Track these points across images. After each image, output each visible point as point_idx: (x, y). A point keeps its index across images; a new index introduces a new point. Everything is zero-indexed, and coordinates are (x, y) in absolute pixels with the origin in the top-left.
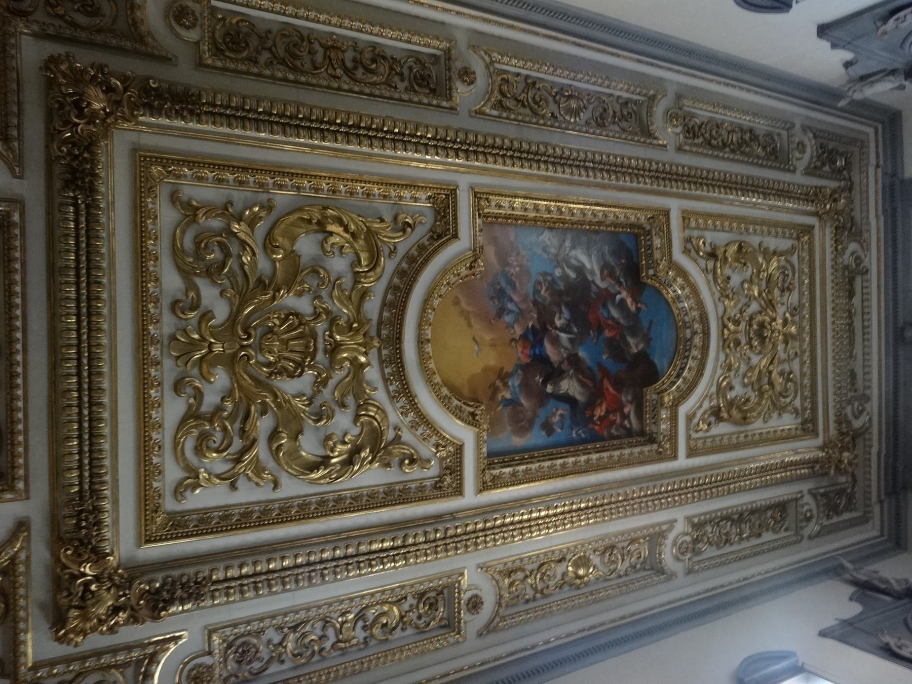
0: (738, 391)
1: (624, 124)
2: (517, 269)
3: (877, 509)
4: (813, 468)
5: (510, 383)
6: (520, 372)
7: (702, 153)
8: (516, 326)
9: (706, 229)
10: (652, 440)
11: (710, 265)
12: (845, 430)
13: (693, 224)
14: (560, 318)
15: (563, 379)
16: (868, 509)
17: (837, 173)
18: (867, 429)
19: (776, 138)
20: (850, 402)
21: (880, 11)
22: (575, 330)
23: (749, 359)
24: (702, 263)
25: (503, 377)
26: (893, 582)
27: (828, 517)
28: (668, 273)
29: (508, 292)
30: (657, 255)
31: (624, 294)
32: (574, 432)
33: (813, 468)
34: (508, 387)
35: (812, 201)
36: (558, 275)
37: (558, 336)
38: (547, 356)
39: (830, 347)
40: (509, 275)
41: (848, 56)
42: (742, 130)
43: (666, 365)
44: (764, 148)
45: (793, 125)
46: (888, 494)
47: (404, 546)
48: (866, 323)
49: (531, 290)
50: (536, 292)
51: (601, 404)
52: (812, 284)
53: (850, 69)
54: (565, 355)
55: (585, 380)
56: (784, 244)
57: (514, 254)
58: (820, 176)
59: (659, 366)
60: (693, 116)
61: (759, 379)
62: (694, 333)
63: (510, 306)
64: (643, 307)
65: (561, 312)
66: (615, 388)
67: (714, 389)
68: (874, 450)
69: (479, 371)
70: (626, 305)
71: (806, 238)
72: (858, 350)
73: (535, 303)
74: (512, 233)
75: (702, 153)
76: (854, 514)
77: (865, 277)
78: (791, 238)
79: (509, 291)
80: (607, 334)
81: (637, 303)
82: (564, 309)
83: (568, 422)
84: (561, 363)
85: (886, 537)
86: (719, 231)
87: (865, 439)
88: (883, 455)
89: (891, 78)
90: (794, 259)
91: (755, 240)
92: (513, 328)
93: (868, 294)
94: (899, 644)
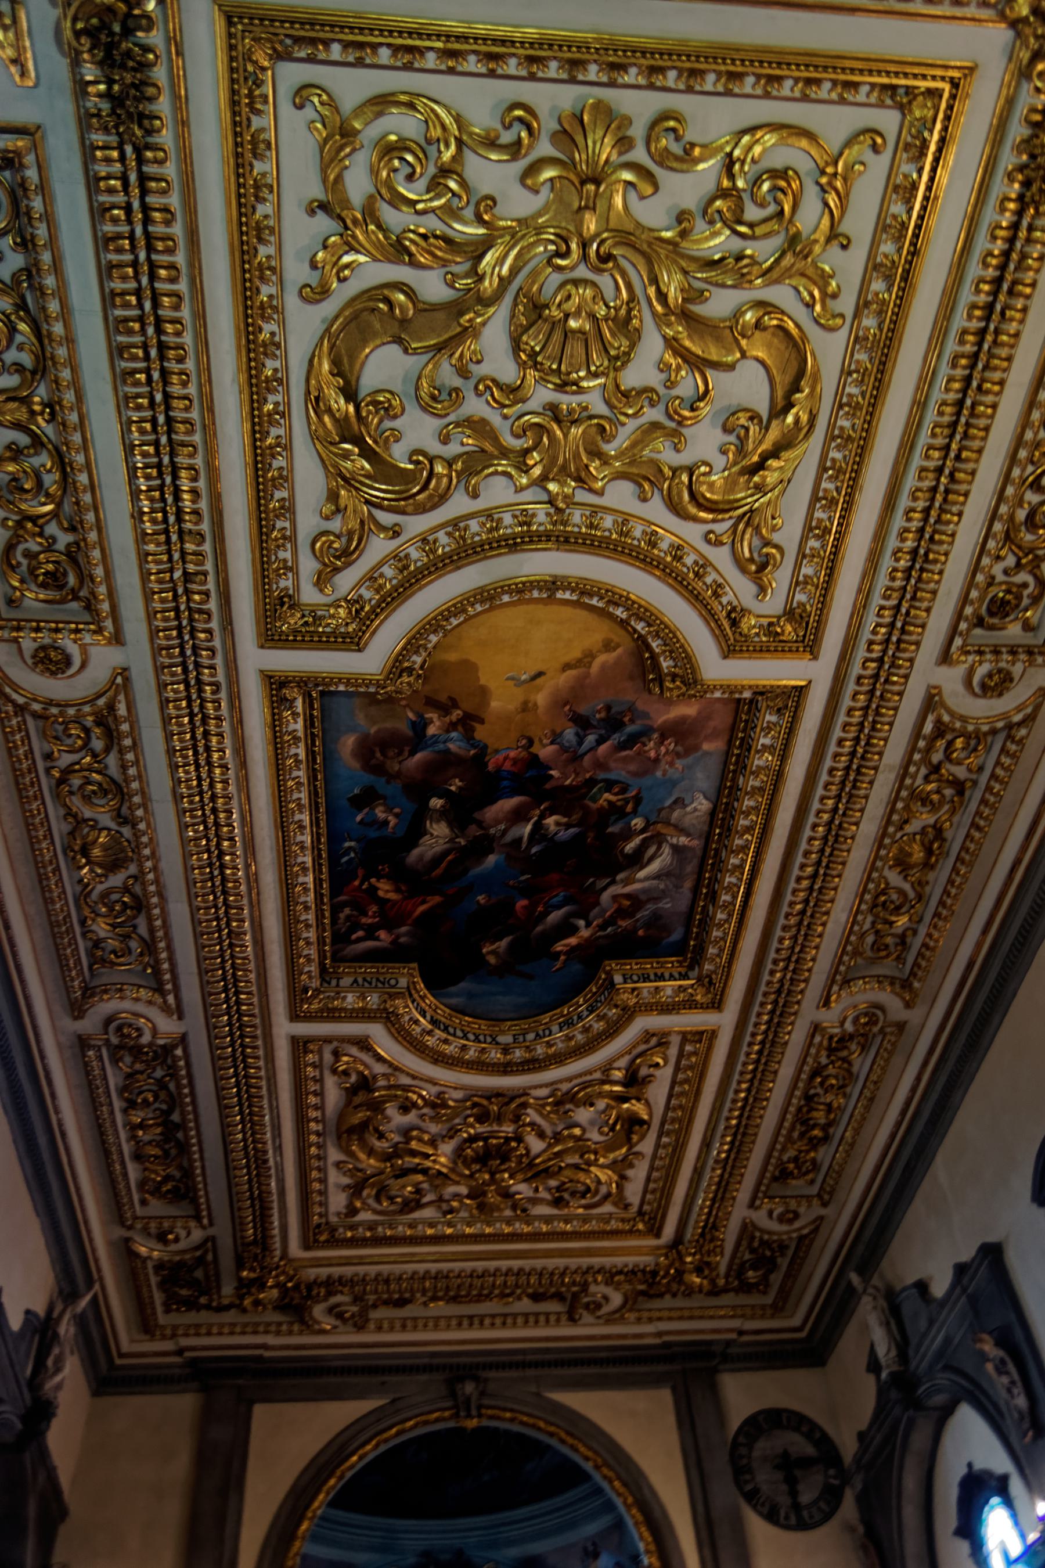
0: (396, 1118)
1: (870, 939)
2: (652, 754)
3: (168, 1346)
4: (255, 1242)
5: (454, 734)
6: (472, 752)
7: (804, 1062)
9: (677, 1069)
11: (618, 1075)
12: (315, 1292)
13: (688, 1048)
14: (558, 824)
15: (450, 825)
16: (168, 1332)
17: (737, 1270)
19: (810, 1176)
20: (357, 1299)
21: (1019, 1335)
22: (534, 850)
23: (451, 1138)
25: (468, 722)
26: (58, 1379)
28: (616, 1006)
29: (616, 736)
31: (585, 933)
32: (353, 844)
34: (448, 731)
35: (702, 1235)
37: (529, 821)
39: (457, 1266)
40: (644, 739)
41: (939, 1289)
42: (830, 1124)
43: (453, 1001)
44: (795, 1160)
45: (825, 1205)
47: (181, 533)
48: (487, 1321)
49: (612, 776)
50: (609, 785)
51: (397, 890)
52: (564, 1236)
53: (914, 1291)
55: (443, 865)
56: (633, 1192)
57: (679, 749)
59: (453, 989)
60: (864, 1048)
61: (414, 1153)
62: (506, 1050)
63: (591, 738)
64: (558, 965)
65: (568, 826)
66: (423, 913)
67: (405, 1080)
68: (271, 1340)
69: (482, 682)
71: (641, 1226)
72: (438, 1308)
73: (592, 782)
75: (804, 1062)
76: (159, 1309)
77: (564, 1318)
78: (642, 1202)
79: (616, 738)
81: (566, 953)
82: (573, 831)
83: (373, 834)
84: (480, 824)
86: (672, 1088)
87: (291, 1323)
89: (893, 1353)
91: (646, 1146)
92: (552, 743)
93: (537, 1322)
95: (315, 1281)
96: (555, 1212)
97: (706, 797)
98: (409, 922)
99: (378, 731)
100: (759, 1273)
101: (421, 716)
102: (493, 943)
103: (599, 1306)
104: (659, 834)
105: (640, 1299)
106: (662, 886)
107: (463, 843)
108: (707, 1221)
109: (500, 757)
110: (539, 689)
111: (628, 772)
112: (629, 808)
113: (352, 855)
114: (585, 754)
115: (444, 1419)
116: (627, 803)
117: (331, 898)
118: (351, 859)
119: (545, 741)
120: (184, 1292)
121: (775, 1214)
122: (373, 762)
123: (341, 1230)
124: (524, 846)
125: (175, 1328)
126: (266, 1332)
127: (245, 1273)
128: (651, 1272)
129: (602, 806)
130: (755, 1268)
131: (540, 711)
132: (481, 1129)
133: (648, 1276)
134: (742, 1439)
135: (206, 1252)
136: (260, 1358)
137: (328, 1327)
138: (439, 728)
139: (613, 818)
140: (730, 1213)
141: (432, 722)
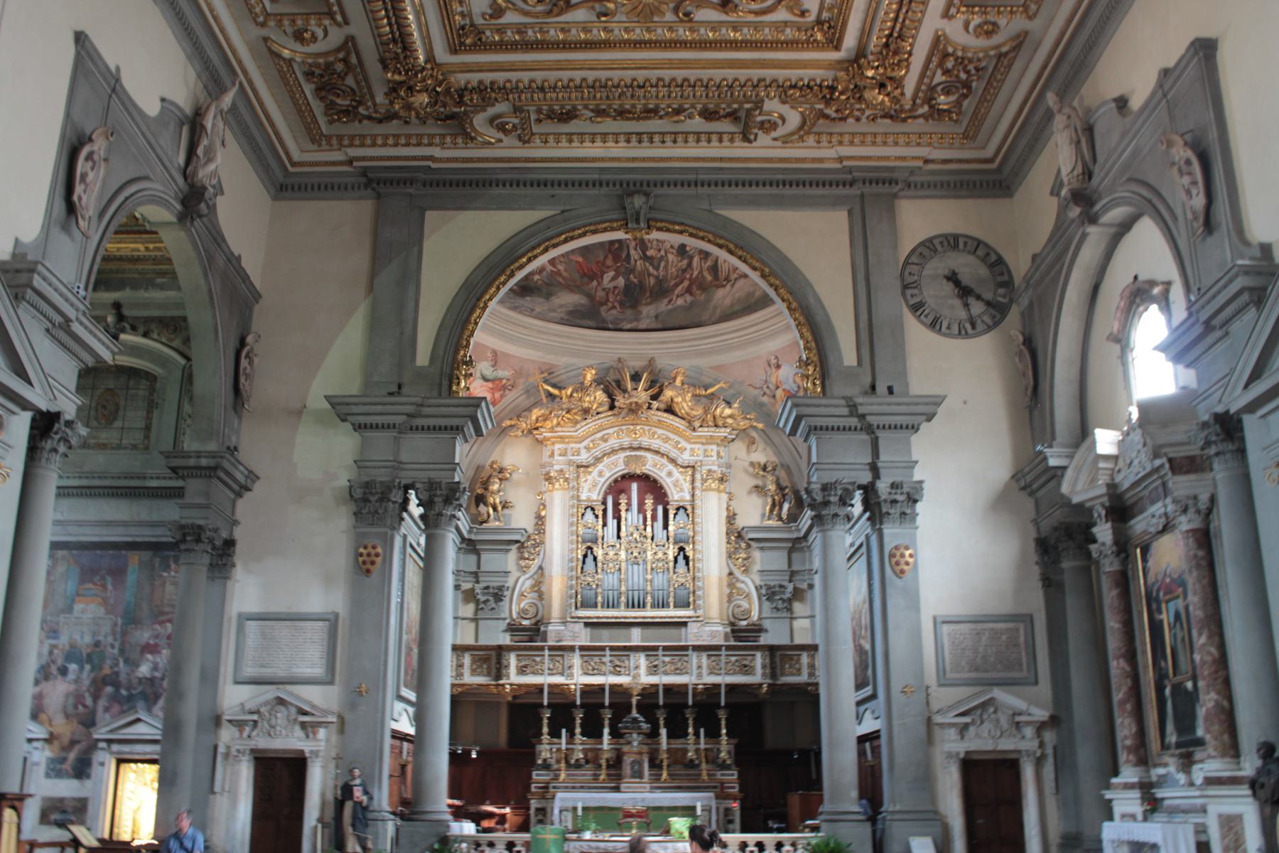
3: (337, 156)
4: (394, 41)
16: (334, 141)
18: (472, 139)
20: (517, 110)
21: (1213, 134)
26: (212, 167)
27: (309, 75)
33: (394, 41)
35: (887, 45)
46: (364, 172)
48: (656, 138)
53: (1113, 105)
58: (928, 61)
68: (437, 152)
71: (819, 36)
72: (609, 125)
76: (322, 120)
77: (738, 138)
85: (290, 169)
87: (455, 136)
88: (429, 163)
89: (1079, 170)
90: (781, 15)
94: (96, 157)
95: (466, 89)
96: (723, 17)
100: (952, 98)
103: (774, 126)
105: (821, 121)
108: (893, 28)
115: (613, 229)
120: (339, 101)
121: (971, 28)
123: (488, 33)
125: (340, 138)
126: (430, 145)
127: (389, 75)
128: (828, 87)
130: (947, 92)
133: (826, 91)
134: (914, 259)
135: (348, 54)
136: (430, 167)
137: (493, 141)
140: (920, 21)
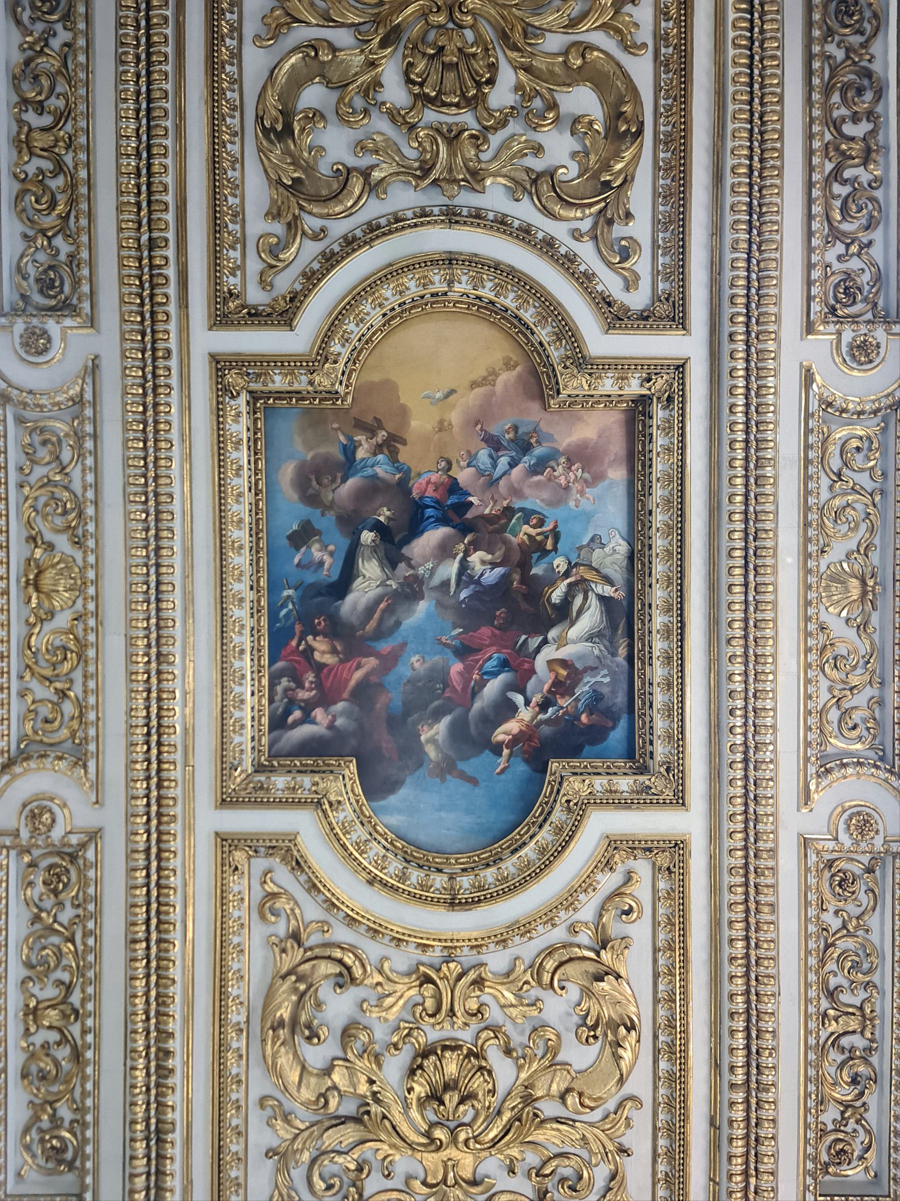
5: (380, 457)
6: (398, 476)
8: (471, 470)
10: (259, 768)
14: (483, 562)
22: (463, 595)
24: (587, 911)
29: (526, 458)
30: (599, 783)
31: (525, 714)
32: (290, 592)
34: (375, 454)
36: (555, 563)
38: (422, 533)
40: (553, 463)
43: (394, 820)
49: (528, 504)
50: (527, 515)
51: (334, 651)
54: (421, 571)
57: (586, 475)
59: (393, 799)
62: (451, 878)
63: (503, 461)
64: (502, 762)
65: (494, 565)
70: (506, 720)
73: (509, 512)
74: (617, 475)
79: (527, 461)
80: (457, 667)
82: (499, 571)
83: (310, 578)
84: (408, 560)
92: (469, 465)
97: (624, 539)
98: (346, 695)
99: (313, 458)
101: (350, 439)
102: (431, 726)
104: (583, 580)
106: (596, 652)
107: (394, 587)
109: (423, 480)
110: (453, 407)
111: (542, 500)
112: (549, 546)
113: (290, 606)
114: (500, 478)
116: (547, 537)
117: (269, 666)
118: (290, 611)
119: (462, 463)
122: (311, 491)
124: (452, 590)
129: (523, 541)
131: (456, 429)
132: (431, 1033)
138: (367, 451)
139: (535, 556)
141: (361, 445)
